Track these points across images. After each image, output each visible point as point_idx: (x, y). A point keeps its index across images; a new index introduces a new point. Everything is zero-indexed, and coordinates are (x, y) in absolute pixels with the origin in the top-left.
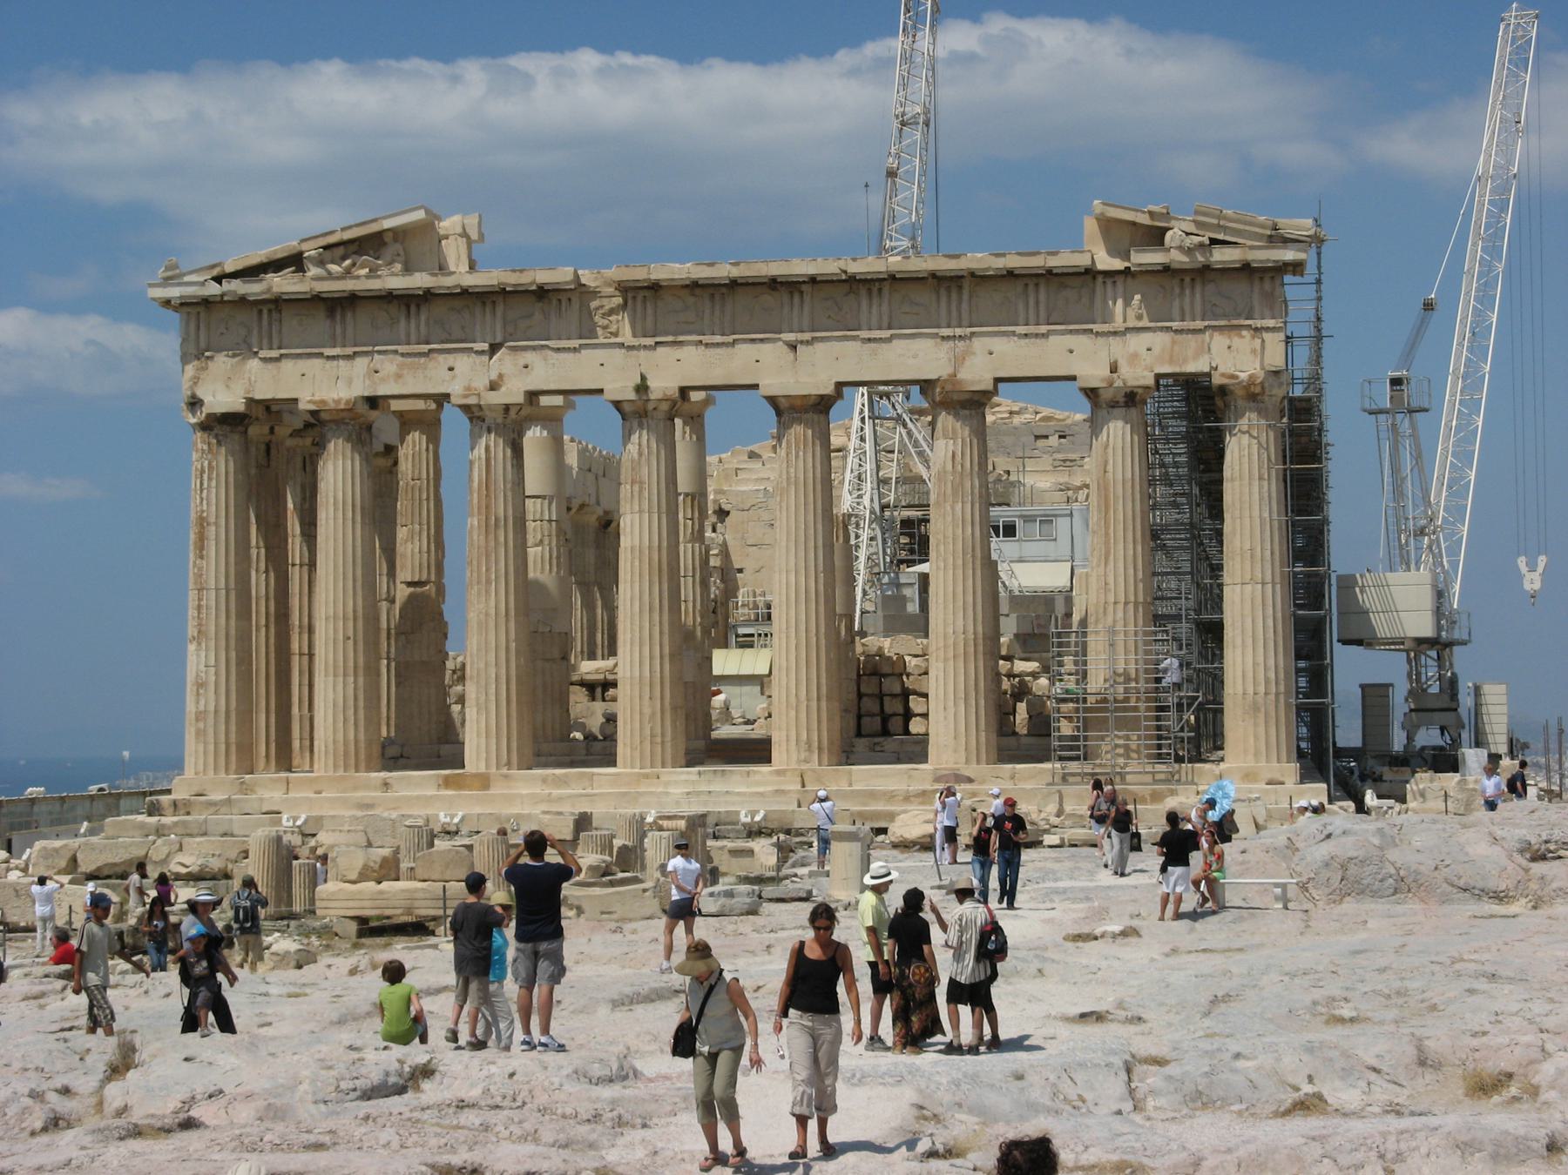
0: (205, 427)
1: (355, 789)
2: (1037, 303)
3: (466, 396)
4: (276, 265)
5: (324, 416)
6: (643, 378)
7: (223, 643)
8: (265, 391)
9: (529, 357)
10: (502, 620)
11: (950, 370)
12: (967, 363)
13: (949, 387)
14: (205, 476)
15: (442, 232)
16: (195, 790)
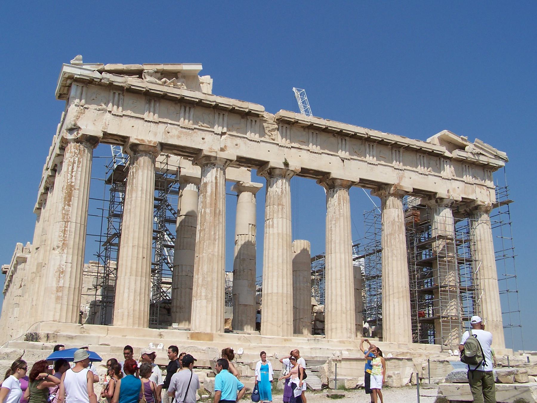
0: (77, 141)
1: (144, 336)
2: (424, 163)
3: (211, 152)
4: (130, 73)
5: (141, 148)
6: (286, 160)
7: (76, 252)
8: (111, 130)
9: (238, 141)
10: (220, 258)
11: (398, 182)
12: (403, 180)
13: (398, 188)
14: (75, 165)
15: (201, 81)
16: (54, 329)
